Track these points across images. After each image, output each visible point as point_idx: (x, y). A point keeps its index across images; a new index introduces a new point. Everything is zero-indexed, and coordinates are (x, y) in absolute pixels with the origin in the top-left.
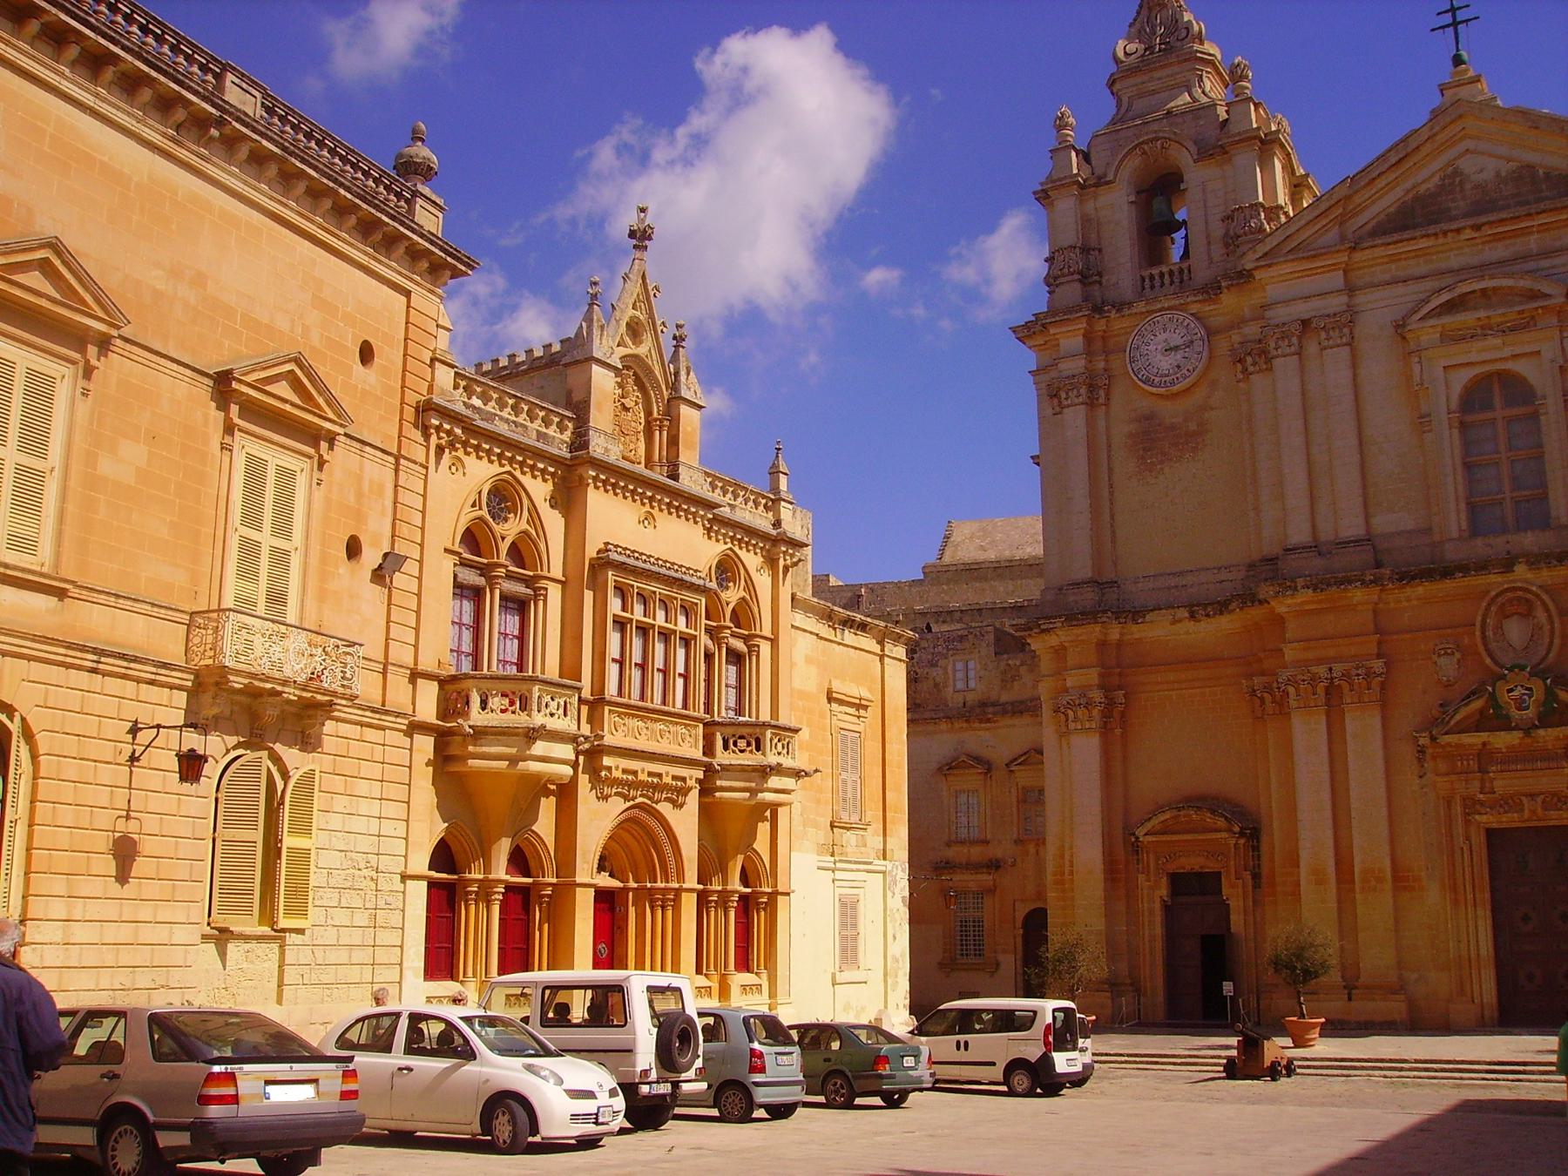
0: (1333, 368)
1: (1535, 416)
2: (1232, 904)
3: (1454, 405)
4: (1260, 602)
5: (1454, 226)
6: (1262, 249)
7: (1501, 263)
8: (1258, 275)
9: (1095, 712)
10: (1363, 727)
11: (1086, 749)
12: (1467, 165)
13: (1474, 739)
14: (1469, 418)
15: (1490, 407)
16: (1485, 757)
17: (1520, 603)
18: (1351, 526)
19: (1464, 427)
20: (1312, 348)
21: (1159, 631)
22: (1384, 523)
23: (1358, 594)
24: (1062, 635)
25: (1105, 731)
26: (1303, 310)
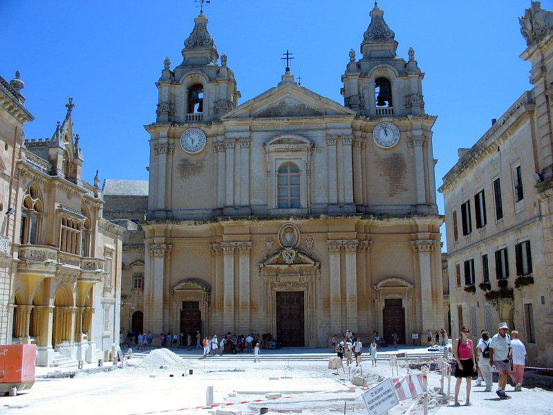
0: (243, 154)
1: (299, 176)
2: (202, 311)
3: (277, 170)
4: (217, 222)
5: (283, 118)
6: (226, 115)
7: (294, 131)
8: (224, 123)
9: (163, 251)
10: (244, 261)
11: (159, 262)
12: (287, 101)
13: (275, 266)
14: (282, 174)
15: (287, 172)
16: (278, 272)
17: (290, 229)
18: (245, 202)
19: (279, 176)
20: (238, 147)
21: (185, 227)
22: (254, 202)
23: (246, 222)
24: (153, 226)
25: (165, 256)
26: (237, 135)
